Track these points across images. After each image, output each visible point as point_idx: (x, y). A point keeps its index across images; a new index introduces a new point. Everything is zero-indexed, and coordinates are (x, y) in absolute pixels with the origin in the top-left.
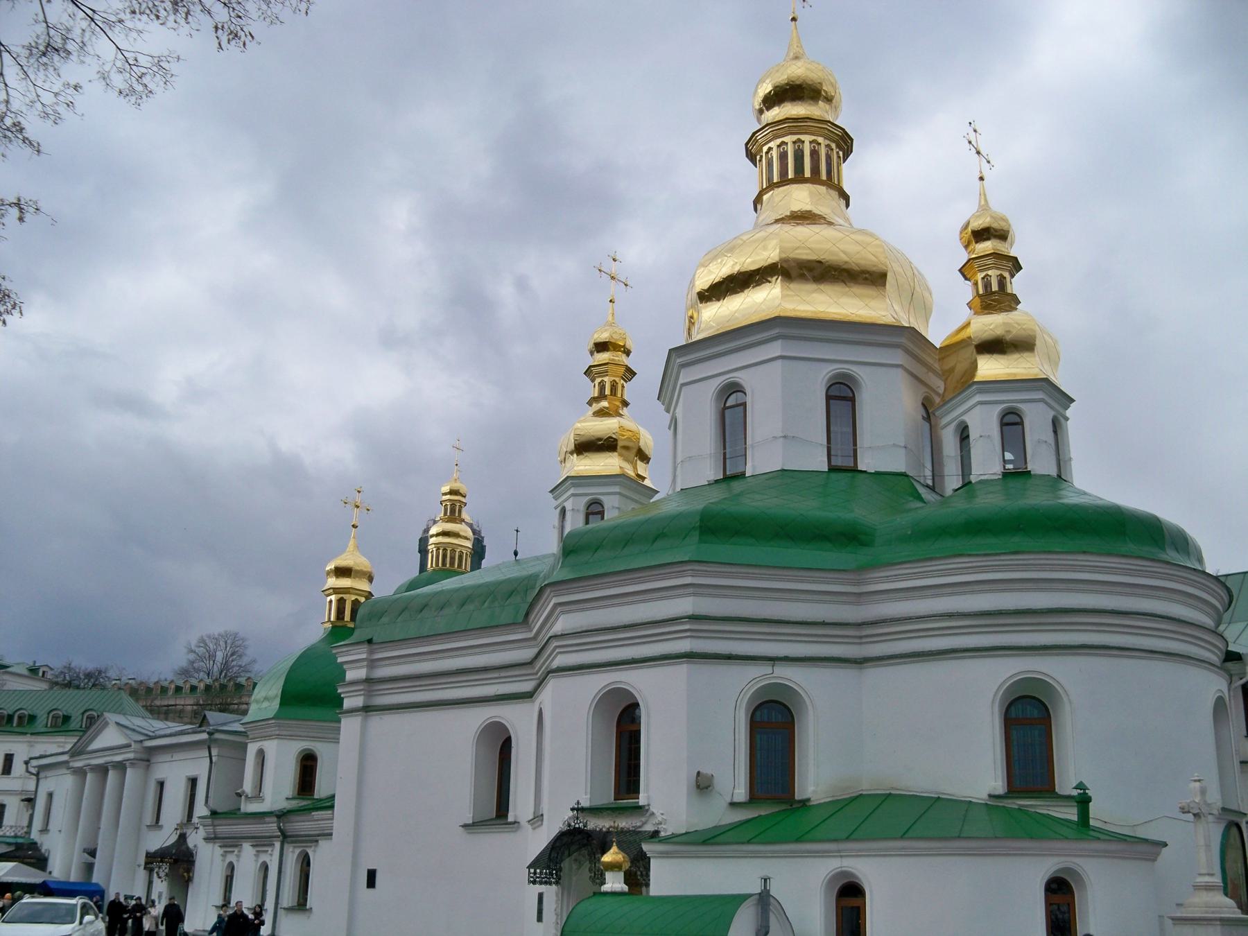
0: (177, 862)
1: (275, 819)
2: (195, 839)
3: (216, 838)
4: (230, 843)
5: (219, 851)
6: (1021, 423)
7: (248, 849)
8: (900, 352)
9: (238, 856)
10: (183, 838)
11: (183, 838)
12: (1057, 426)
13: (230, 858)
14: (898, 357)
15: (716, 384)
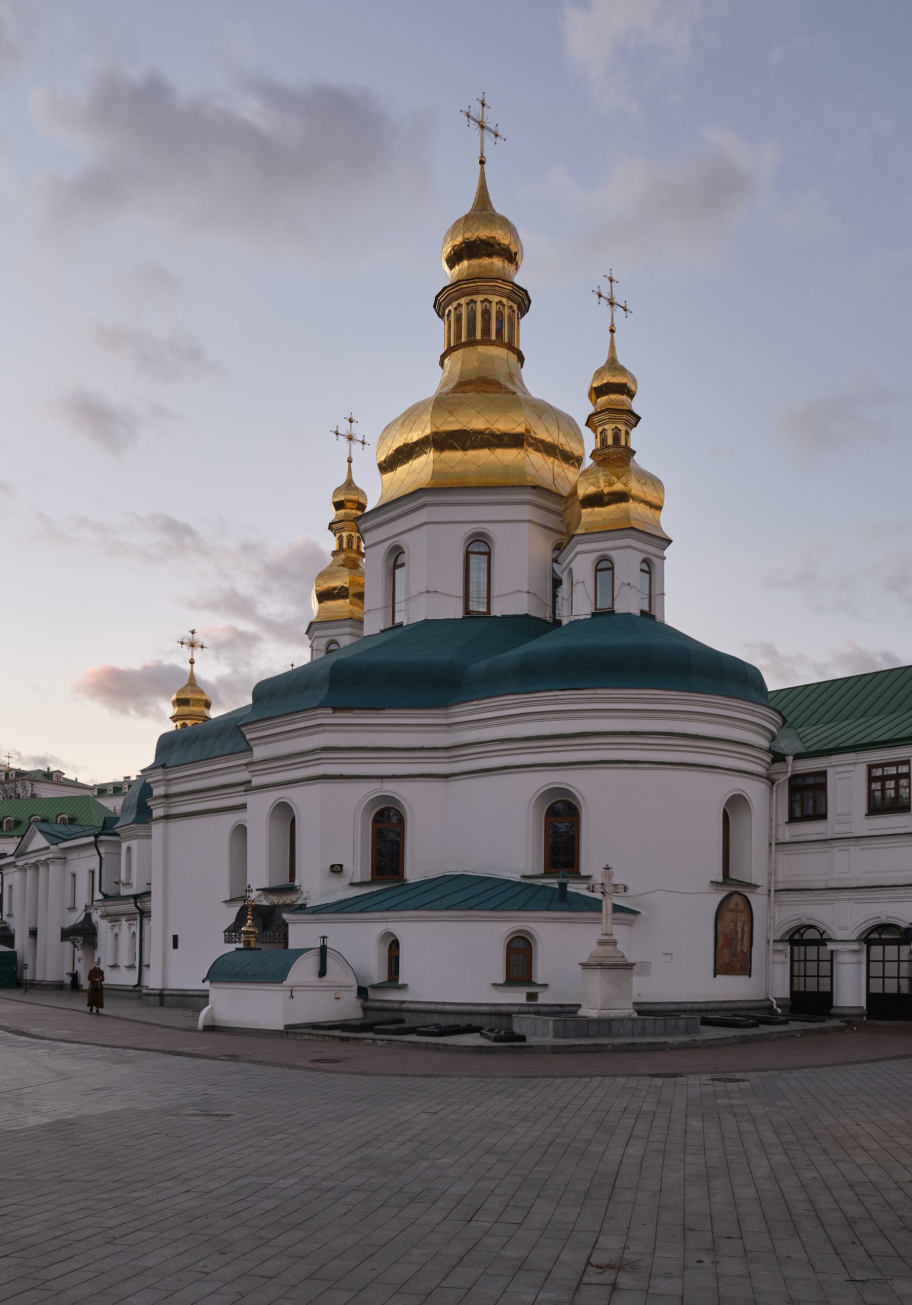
0: (83, 934)
1: (132, 900)
2: (96, 917)
3: (108, 915)
4: (114, 918)
5: (109, 925)
6: (612, 569)
7: (124, 923)
8: (527, 508)
9: (120, 928)
10: (88, 916)
11: (88, 916)
12: (650, 568)
13: (116, 930)
14: (525, 512)
15: (385, 546)
